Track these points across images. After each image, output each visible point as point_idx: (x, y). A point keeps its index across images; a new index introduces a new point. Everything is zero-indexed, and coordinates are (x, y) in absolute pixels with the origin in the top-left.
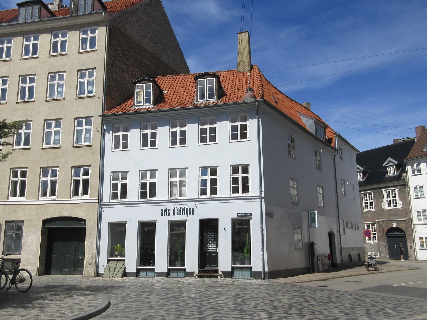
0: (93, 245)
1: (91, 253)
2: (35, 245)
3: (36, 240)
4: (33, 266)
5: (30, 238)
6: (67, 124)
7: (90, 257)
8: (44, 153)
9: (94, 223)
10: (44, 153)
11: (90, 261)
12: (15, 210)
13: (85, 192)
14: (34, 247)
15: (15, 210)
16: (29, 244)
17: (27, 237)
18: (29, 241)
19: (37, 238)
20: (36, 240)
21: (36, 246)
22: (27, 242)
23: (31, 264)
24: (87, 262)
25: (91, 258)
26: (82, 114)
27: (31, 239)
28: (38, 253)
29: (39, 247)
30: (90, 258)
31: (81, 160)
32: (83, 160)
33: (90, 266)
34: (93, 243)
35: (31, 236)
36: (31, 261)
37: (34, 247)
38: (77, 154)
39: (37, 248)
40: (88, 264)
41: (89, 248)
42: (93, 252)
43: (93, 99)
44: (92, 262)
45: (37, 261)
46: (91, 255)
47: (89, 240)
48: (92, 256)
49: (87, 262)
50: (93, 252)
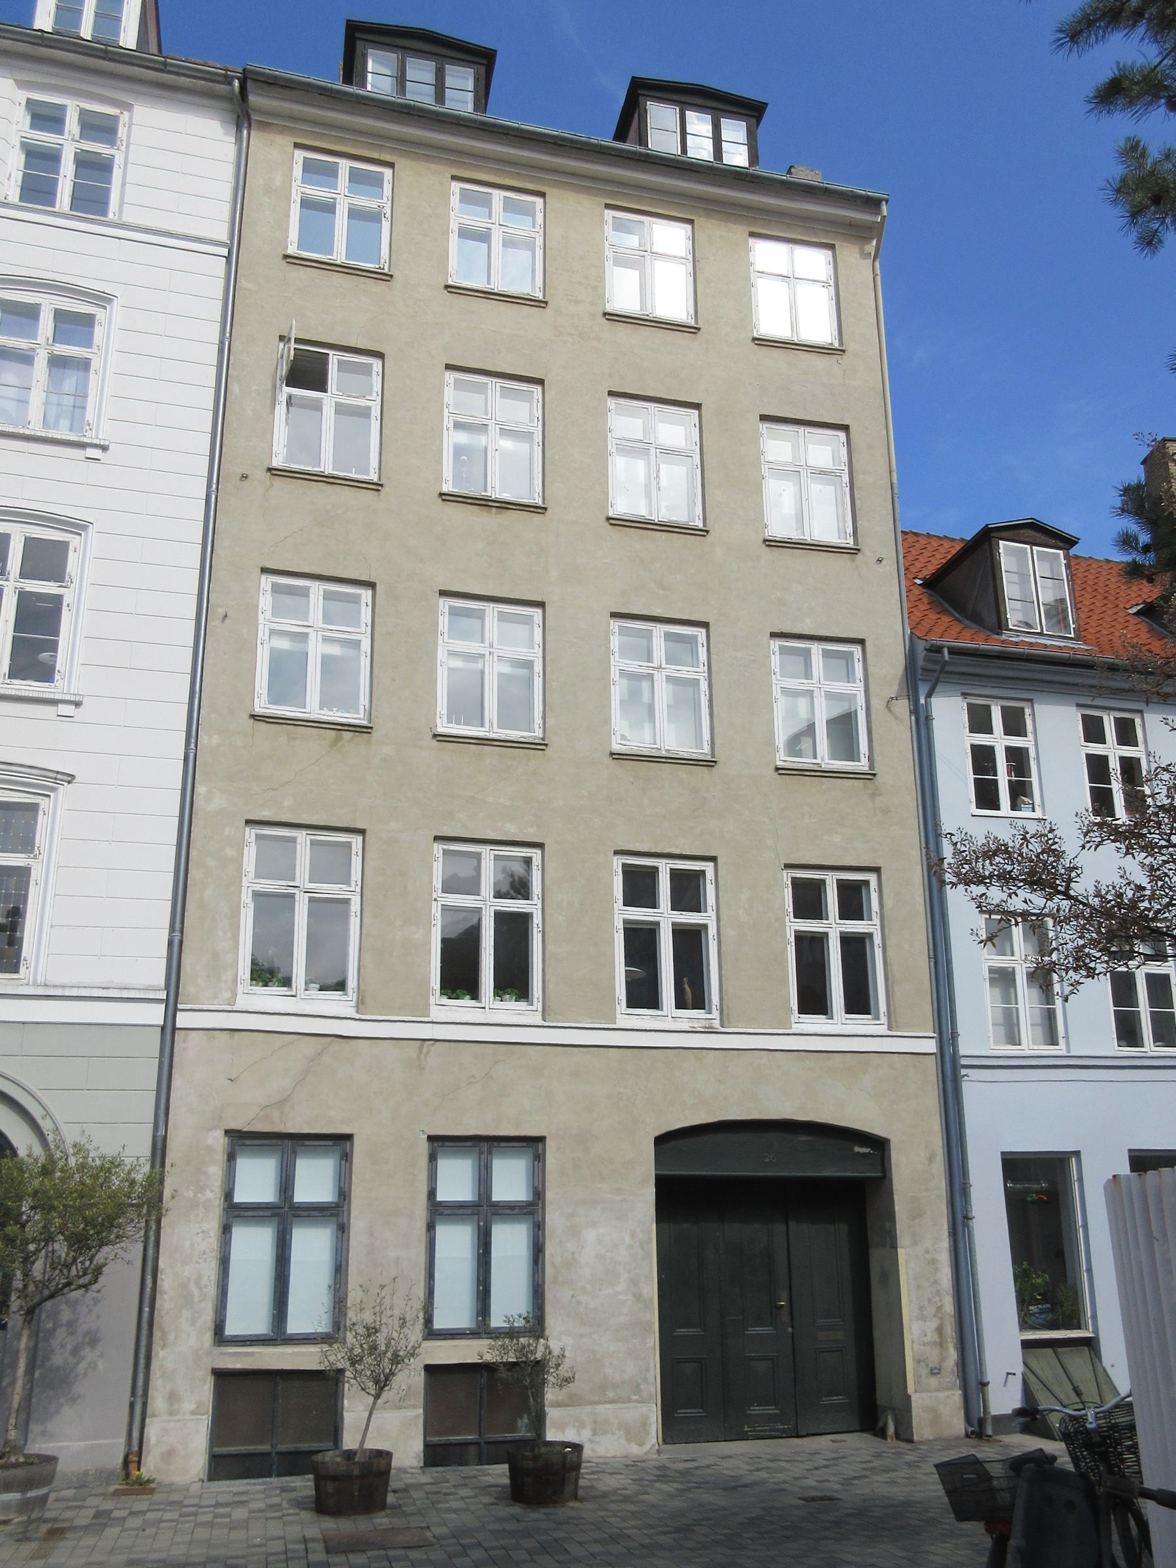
0: (937, 1269)
1: (930, 1311)
3: (630, 1247)
5: (590, 1235)
7: (929, 1334)
8: (631, 780)
9: (931, 1159)
11: (933, 1356)
13: (859, 1002)
14: (621, 1287)
17: (574, 1232)
19: (633, 1235)
20: (630, 1247)
21: (634, 1282)
22: (571, 1263)
23: (615, 1386)
24: (919, 1361)
25: (936, 1338)
29: (651, 1290)
30: (929, 1339)
31: (826, 838)
32: (837, 839)
33: (933, 1382)
34: (934, 1261)
35: (594, 1224)
36: (608, 1371)
37: (621, 1287)
39: (638, 1297)
40: (924, 1372)
41: (918, 1287)
42: (939, 1309)
44: (943, 1359)
45: (648, 1370)
46: (933, 1324)
47: (915, 1243)
48: (940, 1330)
49: (919, 1361)
50: (939, 1309)
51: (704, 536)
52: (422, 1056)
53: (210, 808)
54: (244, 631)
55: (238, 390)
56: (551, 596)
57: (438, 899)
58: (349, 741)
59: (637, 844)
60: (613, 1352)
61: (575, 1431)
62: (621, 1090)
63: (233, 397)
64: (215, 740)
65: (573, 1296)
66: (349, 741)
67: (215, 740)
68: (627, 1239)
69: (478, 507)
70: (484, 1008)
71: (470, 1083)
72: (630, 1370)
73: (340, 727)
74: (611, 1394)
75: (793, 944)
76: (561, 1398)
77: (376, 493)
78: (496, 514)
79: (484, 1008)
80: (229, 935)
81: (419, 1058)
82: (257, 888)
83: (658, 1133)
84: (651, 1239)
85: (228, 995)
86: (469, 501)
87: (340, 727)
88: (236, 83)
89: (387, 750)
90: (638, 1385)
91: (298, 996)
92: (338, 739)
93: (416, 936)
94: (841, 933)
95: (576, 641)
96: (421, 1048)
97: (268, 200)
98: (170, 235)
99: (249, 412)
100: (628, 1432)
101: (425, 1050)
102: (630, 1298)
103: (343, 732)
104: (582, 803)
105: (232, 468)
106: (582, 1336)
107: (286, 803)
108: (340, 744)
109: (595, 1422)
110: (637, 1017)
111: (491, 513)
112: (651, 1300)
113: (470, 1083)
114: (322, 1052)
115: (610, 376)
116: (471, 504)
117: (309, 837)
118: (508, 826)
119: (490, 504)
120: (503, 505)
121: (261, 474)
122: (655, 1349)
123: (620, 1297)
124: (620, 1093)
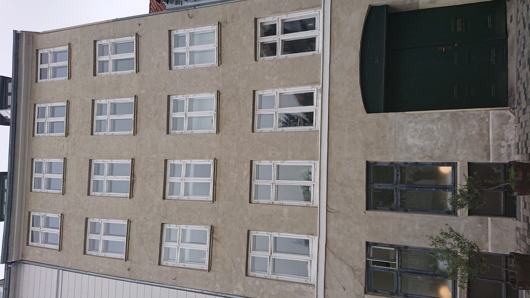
2: (429, 125)
3: (416, 123)
4: (488, 123)
5: (410, 141)
6: (178, 82)
8: (226, 126)
10: (226, 126)
12: (341, 184)
14: (435, 127)
15: (341, 184)
16: (427, 142)
17: (408, 148)
18: (420, 143)
19: (411, 122)
20: (416, 123)
21: (432, 121)
22: (423, 149)
23: (481, 130)
26: (164, 54)
27: (413, 137)
28: (451, 114)
29: (436, 113)
35: (405, 140)
37: (435, 127)
38: (233, 52)
39: (439, 119)
43: (141, 36)
45: (474, 114)
51: (137, 97)
52: (333, 211)
53: (242, 290)
54: (180, 272)
55: (102, 270)
56: (163, 157)
57: (273, 202)
58: (216, 234)
59: (250, 123)
60: (465, 130)
61: (502, 149)
62: (346, 129)
63: (104, 272)
64: (218, 286)
65: (438, 149)
66: (216, 234)
67: (218, 286)
68: (412, 125)
69: (134, 184)
70: (314, 185)
71: (344, 192)
72: (474, 122)
73: (212, 239)
74: (485, 132)
75: (286, 55)
76: (486, 155)
77: (131, 222)
78: (136, 178)
79: (314, 185)
80: (288, 286)
81: (334, 213)
82: (270, 273)
83: (365, 112)
84: (413, 114)
85: (311, 288)
86: (132, 188)
87: (212, 239)
88: (9, 266)
89: (219, 221)
90: (481, 118)
91: (311, 259)
92: (216, 239)
93: (286, 212)
94: (282, 34)
95: (178, 148)
96: (329, 211)
97: (44, 255)
98: (57, 290)
99: (108, 267)
100: (504, 124)
101: (331, 210)
102: (440, 123)
103: (213, 237)
104: (235, 145)
105: (127, 274)
106: (457, 145)
107: (239, 260)
108: (218, 239)
109: (498, 139)
110: (316, 122)
111: (136, 180)
112: (441, 113)
113: (344, 192)
114: (332, 252)
115: (86, 135)
116: (133, 187)
117: (252, 252)
118: (244, 174)
119: (132, 180)
120: (132, 175)
121: (128, 263)
122: (464, 111)
123: (439, 127)
124: (348, 129)
